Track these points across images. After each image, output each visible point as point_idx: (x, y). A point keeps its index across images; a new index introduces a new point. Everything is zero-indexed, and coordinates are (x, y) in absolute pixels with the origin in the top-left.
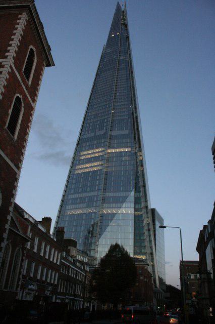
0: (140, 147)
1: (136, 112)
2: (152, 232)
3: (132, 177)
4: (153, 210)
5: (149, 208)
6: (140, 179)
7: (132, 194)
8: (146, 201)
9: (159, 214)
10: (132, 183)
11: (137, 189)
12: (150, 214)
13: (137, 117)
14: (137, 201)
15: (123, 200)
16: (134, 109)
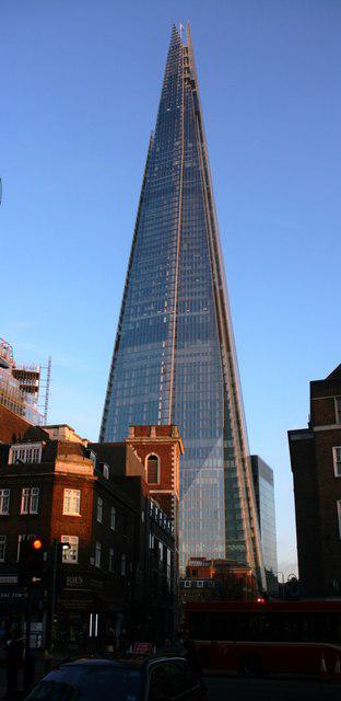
0: (229, 350)
1: (220, 284)
2: (252, 504)
3: (220, 415)
4: (254, 459)
5: (246, 455)
6: (232, 415)
7: (220, 443)
8: (242, 449)
9: (265, 465)
10: (220, 424)
11: (227, 435)
12: (248, 464)
13: (221, 292)
14: (228, 454)
15: (207, 452)
16: (216, 280)
